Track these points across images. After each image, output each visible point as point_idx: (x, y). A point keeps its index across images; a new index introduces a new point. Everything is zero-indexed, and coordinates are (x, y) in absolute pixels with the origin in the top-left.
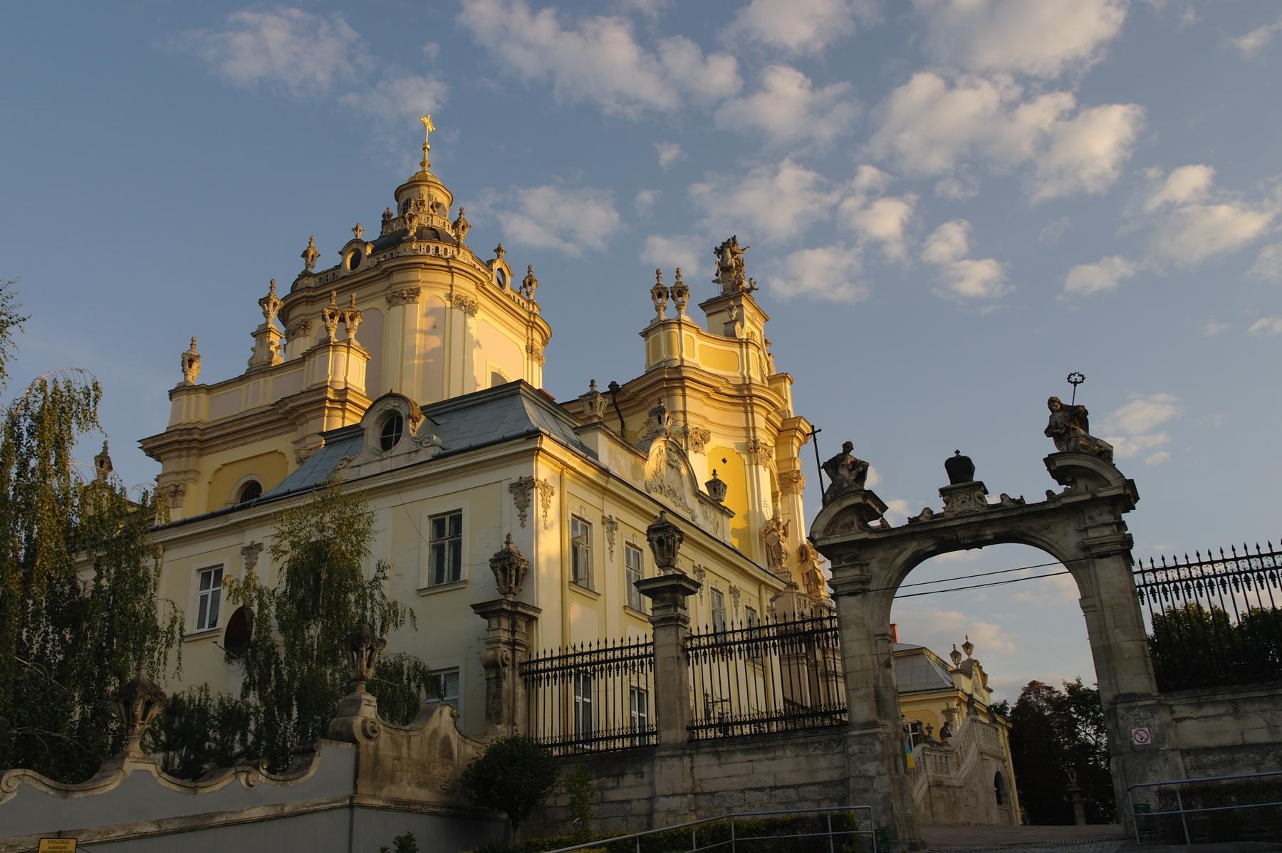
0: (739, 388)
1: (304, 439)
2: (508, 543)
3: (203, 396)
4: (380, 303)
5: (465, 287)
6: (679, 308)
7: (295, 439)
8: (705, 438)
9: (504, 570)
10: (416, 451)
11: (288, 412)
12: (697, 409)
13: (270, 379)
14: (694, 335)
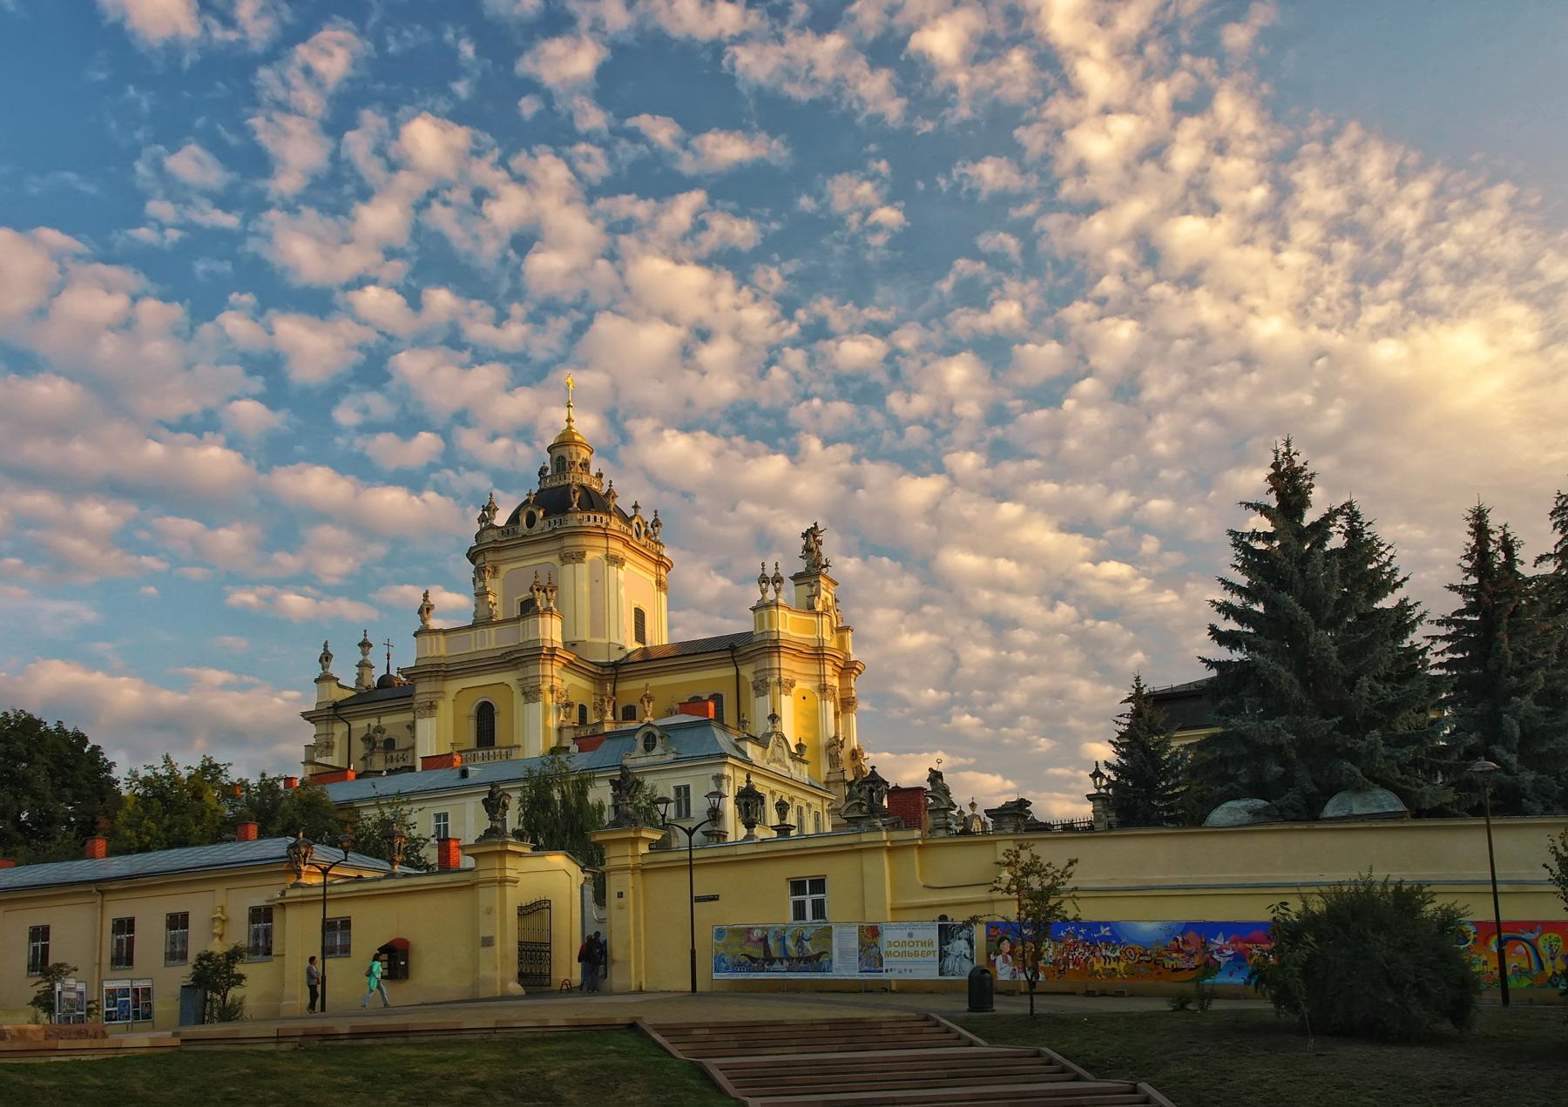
0: (816, 649)
3: (441, 637)
4: (554, 559)
5: (616, 547)
6: (777, 591)
8: (792, 685)
12: (788, 666)
13: (493, 630)
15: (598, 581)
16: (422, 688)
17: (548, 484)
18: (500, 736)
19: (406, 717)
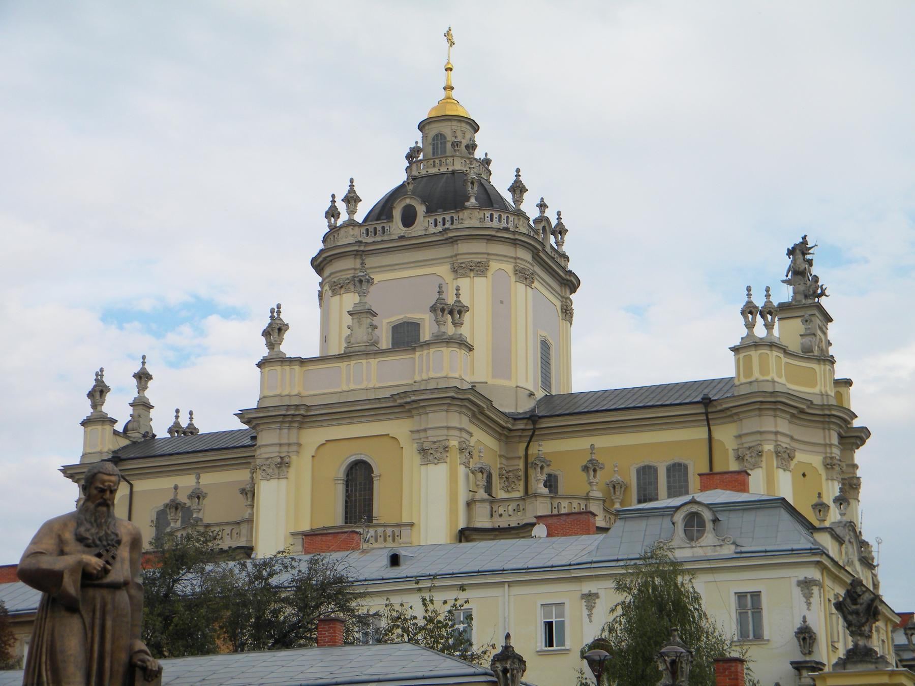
0: (822, 407)
1: (425, 430)
2: (805, 621)
3: (297, 368)
4: (443, 270)
7: (415, 429)
9: (804, 639)
10: (720, 546)
13: (374, 362)
14: (782, 355)
15: (501, 302)
16: (268, 437)
17: (423, 170)
18: (381, 508)
19: (241, 476)
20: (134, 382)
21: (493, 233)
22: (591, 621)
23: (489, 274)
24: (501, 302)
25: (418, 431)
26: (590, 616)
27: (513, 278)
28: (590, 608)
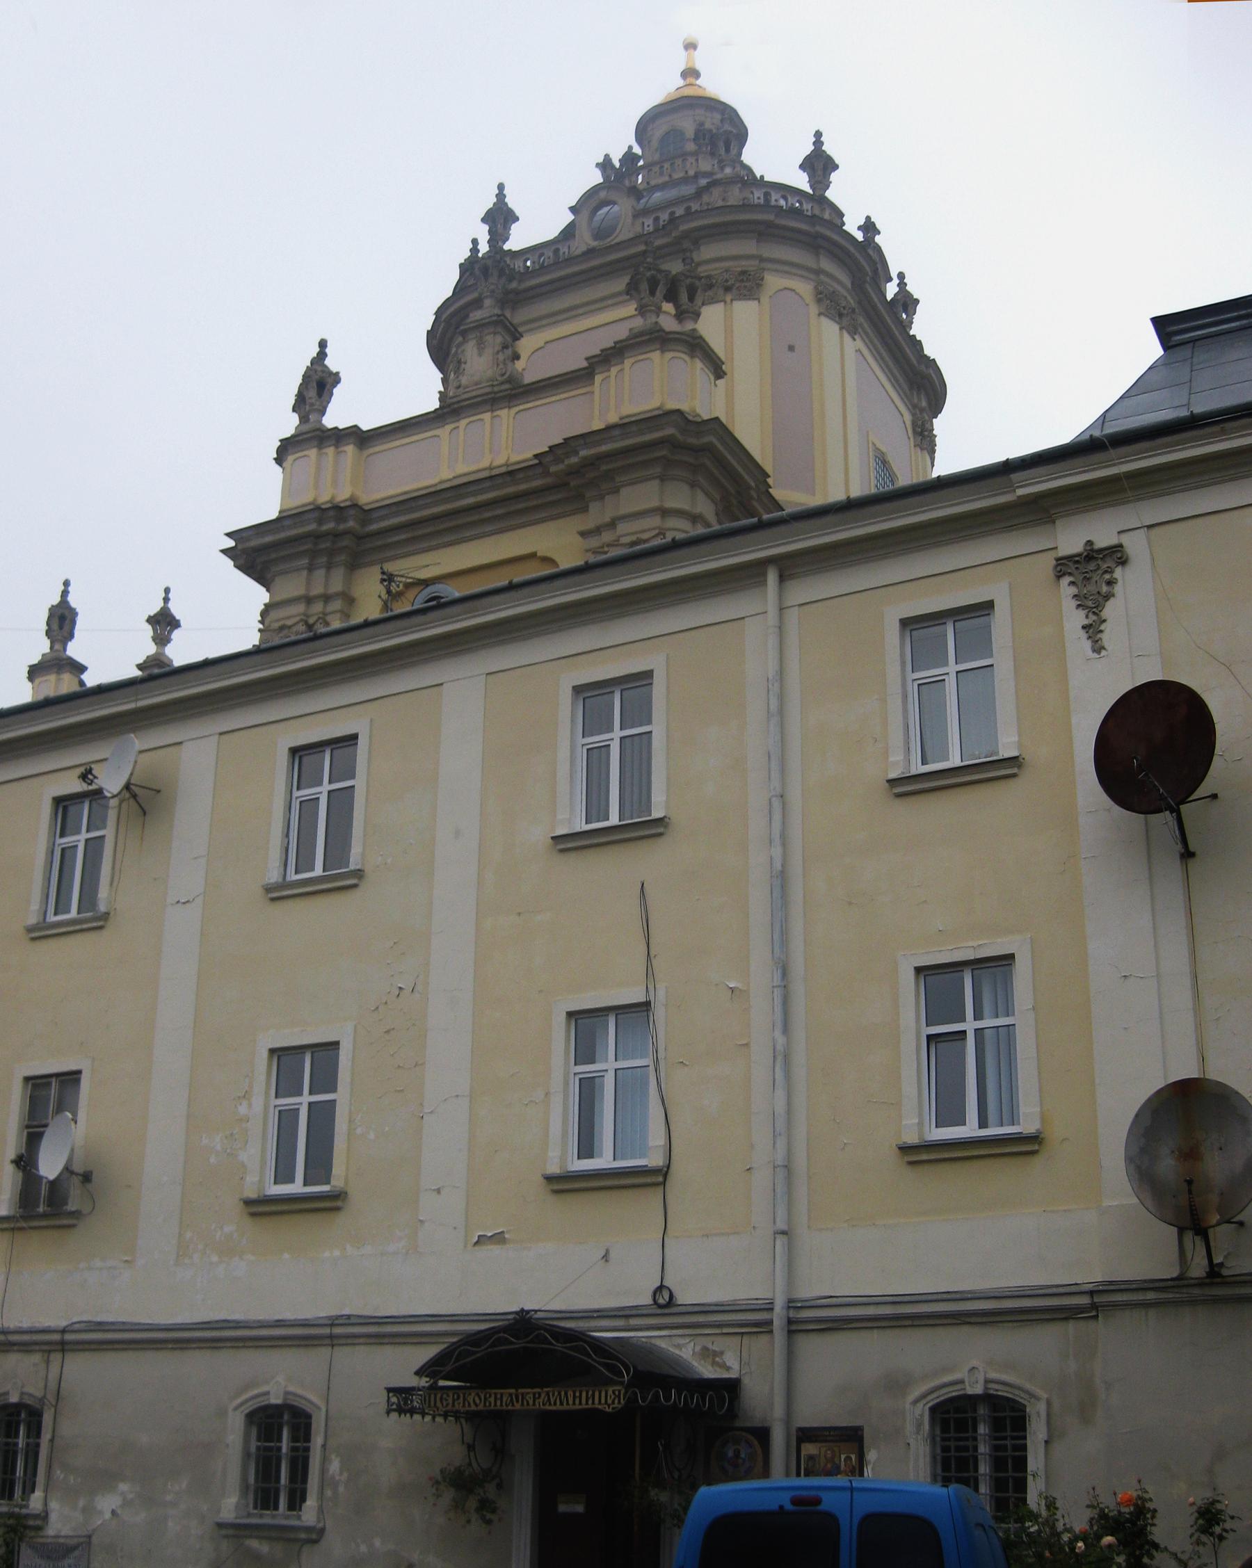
1: (612, 524)
3: (350, 449)
11: (574, 472)
13: (503, 413)
20: (148, 631)
21: (771, 217)
22: (1098, 648)
23: (765, 299)
24: (788, 350)
25: (597, 530)
26: (1093, 630)
27: (814, 309)
28: (1094, 605)
